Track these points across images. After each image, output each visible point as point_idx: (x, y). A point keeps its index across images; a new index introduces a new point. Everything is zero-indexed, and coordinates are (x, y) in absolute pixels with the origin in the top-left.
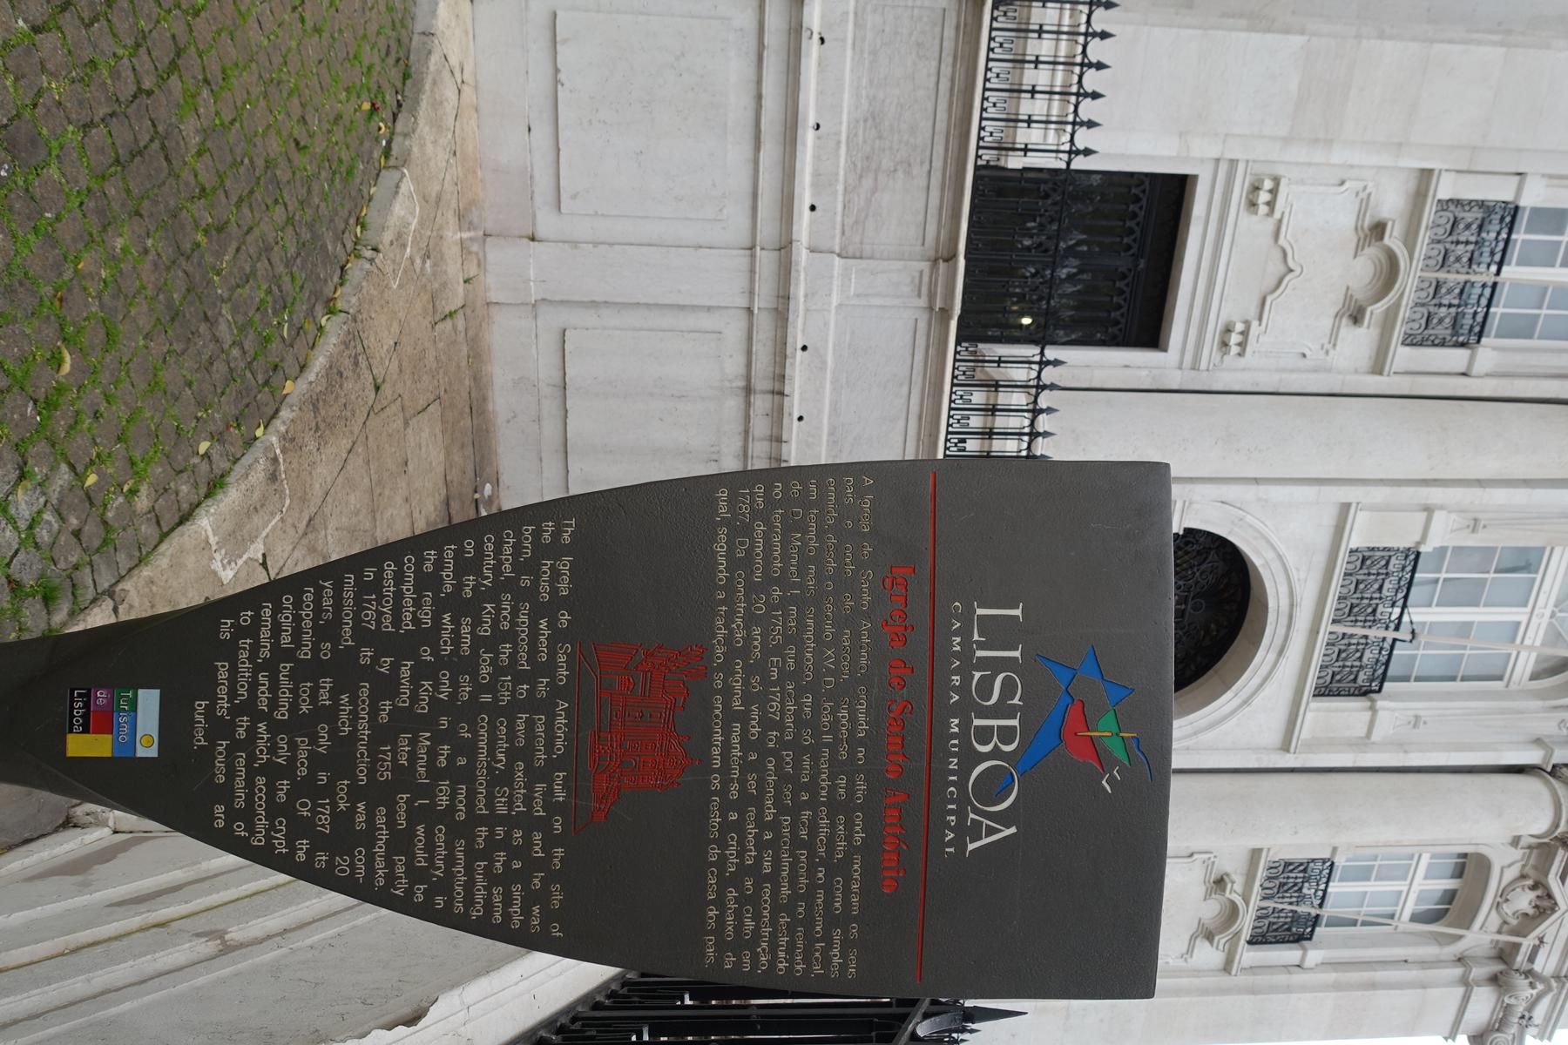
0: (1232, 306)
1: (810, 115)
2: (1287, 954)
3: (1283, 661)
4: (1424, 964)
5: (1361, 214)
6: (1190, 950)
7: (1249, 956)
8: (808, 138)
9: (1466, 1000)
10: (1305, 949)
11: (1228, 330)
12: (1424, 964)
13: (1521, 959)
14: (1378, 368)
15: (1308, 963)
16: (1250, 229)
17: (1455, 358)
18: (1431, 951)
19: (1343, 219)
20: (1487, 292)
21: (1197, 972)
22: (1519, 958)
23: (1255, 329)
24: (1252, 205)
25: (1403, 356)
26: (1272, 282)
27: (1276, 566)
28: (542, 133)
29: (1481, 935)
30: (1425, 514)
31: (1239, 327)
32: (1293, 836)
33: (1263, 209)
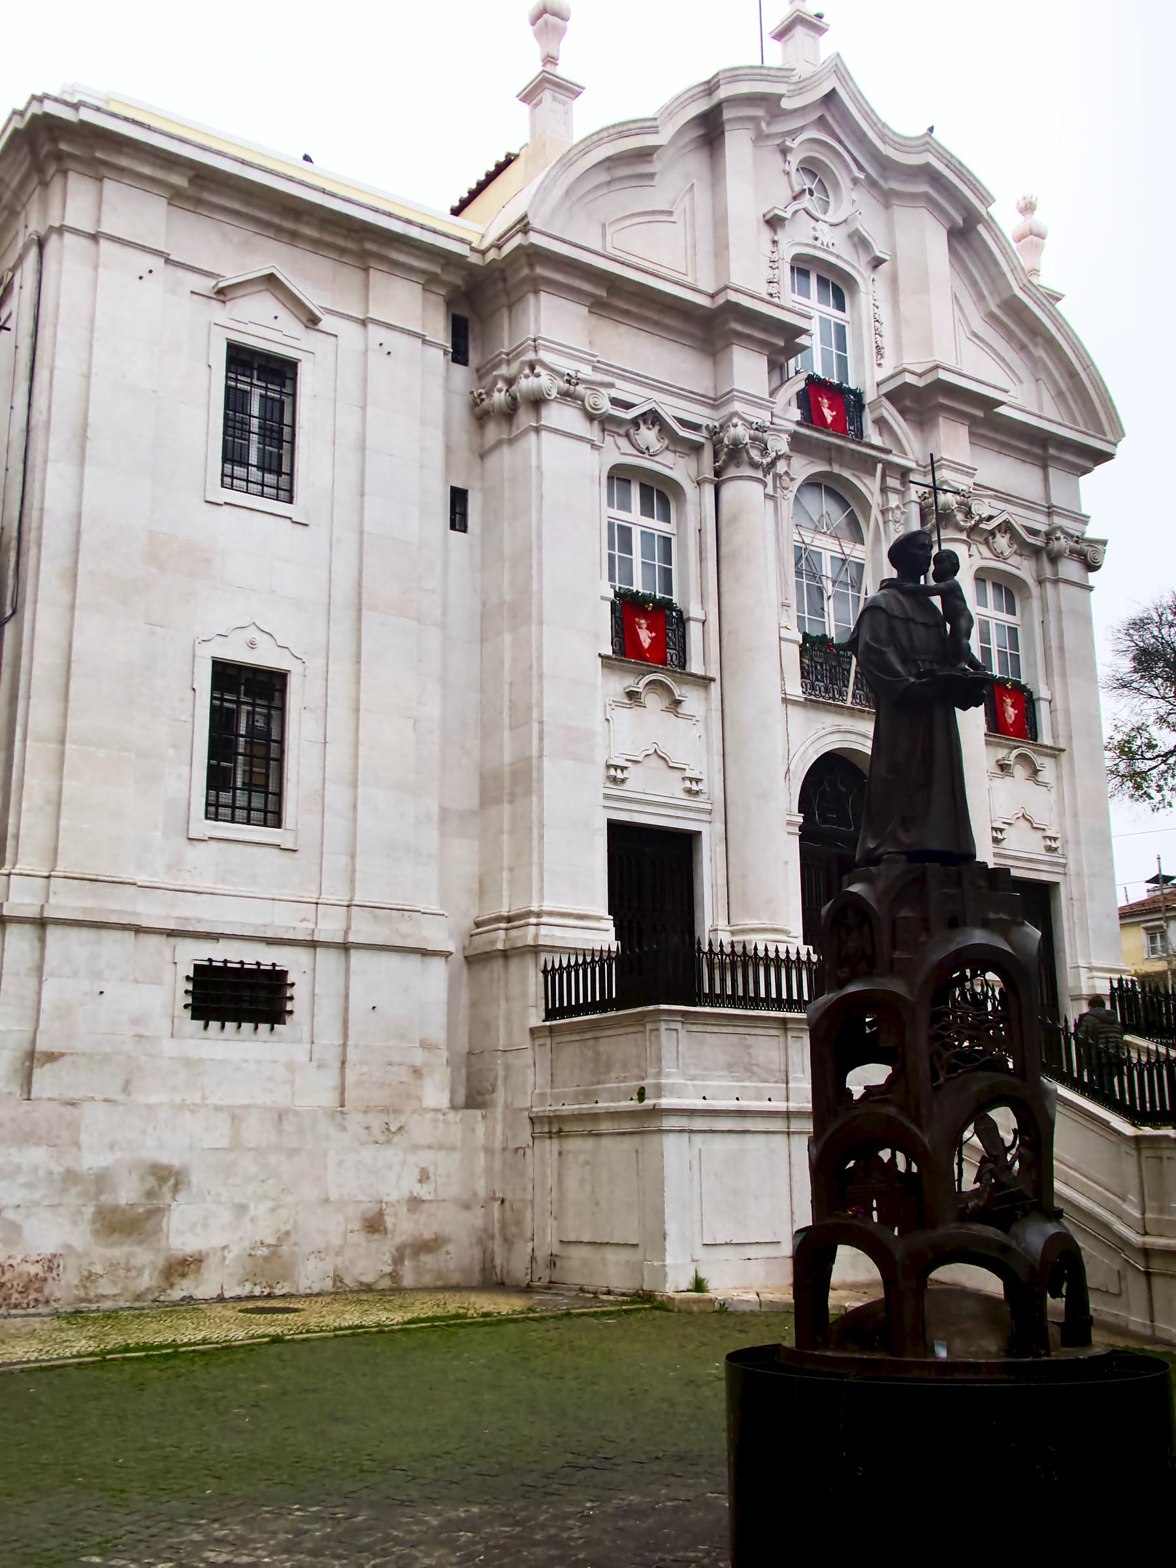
0: (673, 788)
1: (731, 1104)
2: (1043, 710)
4: (1044, 610)
5: (623, 706)
6: (1045, 785)
7: (1046, 738)
8: (745, 1104)
9: (1067, 582)
10: (1039, 699)
11: (689, 791)
12: (1044, 610)
13: (1038, 542)
16: (637, 781)
17: (694, 630)
18: (1035, 604)
19: (625, 717)
21: (1059, 778)
22: (1039, 543)
23: (688, 774)
24: (623, 781)
25: (695, 666)
26: (661, 762)
27: (817, 745)
28: (751, 1252)
29: (1024, 569)
31: (688, 784)
33: (626, 774)
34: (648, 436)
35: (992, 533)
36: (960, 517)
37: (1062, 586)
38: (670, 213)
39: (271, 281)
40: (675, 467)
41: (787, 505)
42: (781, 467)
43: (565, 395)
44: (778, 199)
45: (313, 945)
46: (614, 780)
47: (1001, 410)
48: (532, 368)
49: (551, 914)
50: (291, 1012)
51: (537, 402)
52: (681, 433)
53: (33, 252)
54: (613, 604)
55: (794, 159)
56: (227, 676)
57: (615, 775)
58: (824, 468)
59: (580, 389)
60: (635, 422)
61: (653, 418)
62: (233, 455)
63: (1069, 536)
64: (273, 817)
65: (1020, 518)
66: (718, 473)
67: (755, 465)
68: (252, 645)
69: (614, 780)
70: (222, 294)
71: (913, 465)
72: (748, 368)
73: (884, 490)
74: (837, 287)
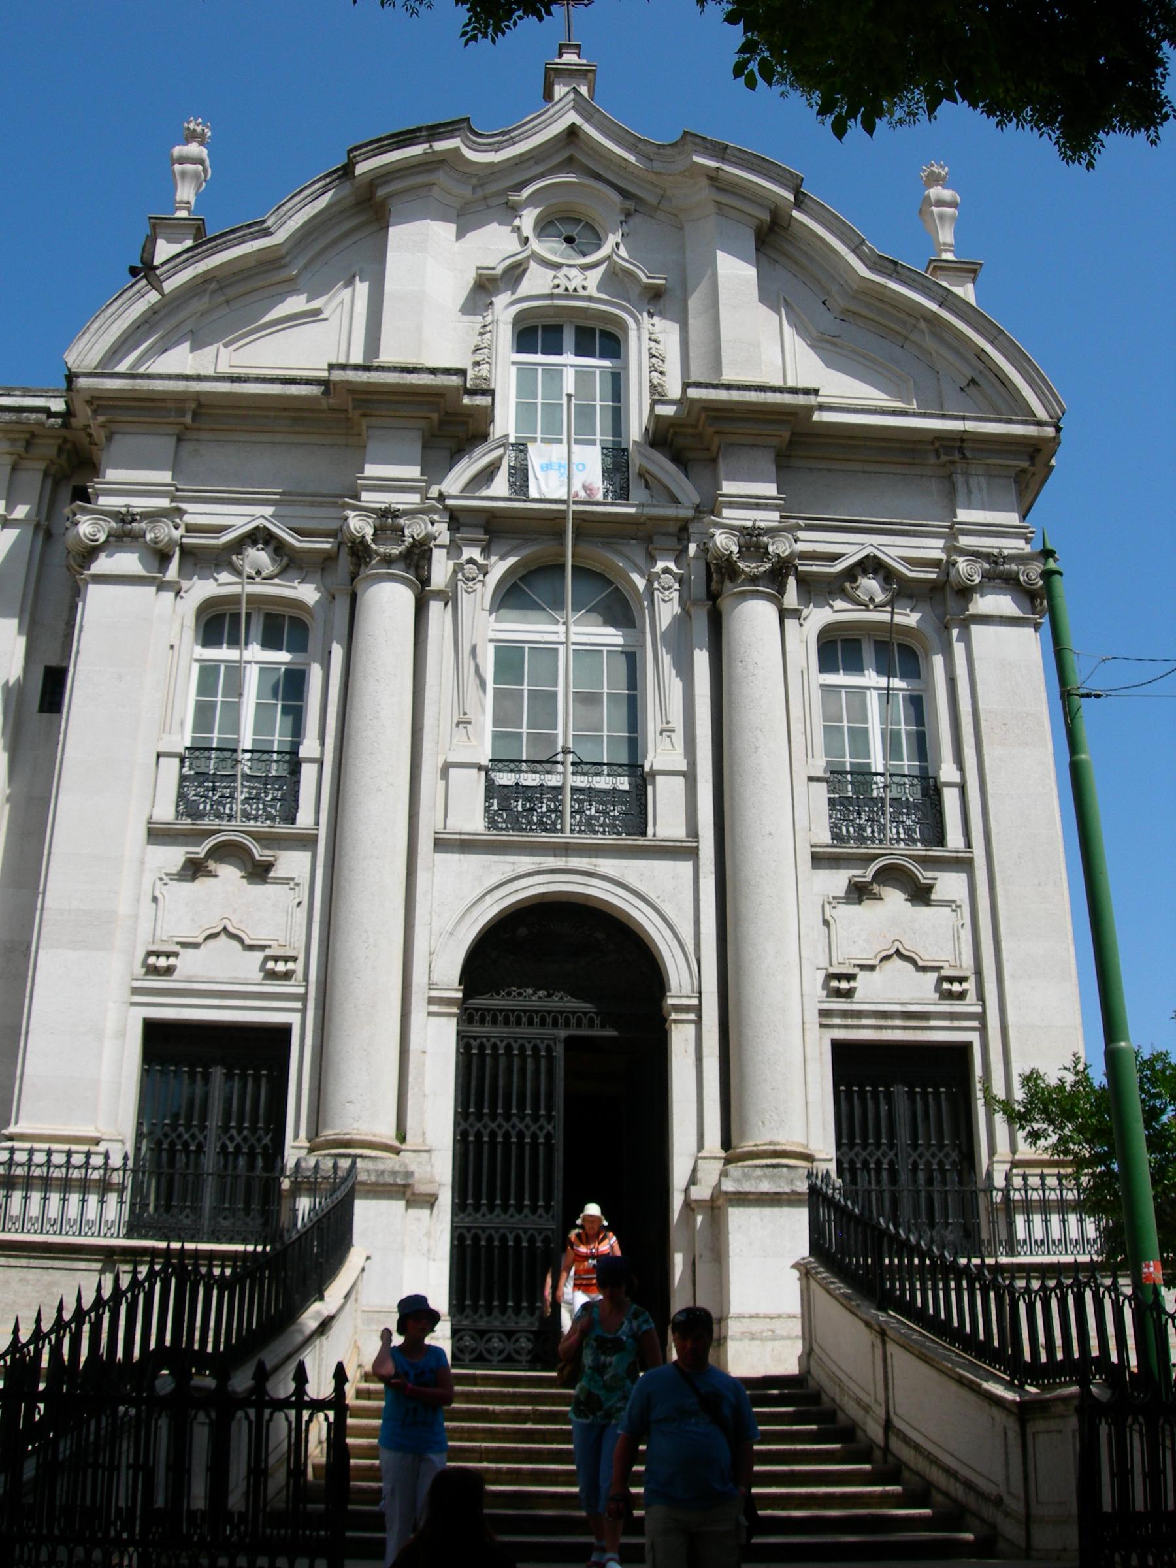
2: (950, 798)
7: (954, 839)
11: (271, 975)
14: (306, 842)
15: (956, 777)
20: (257, 755)
25: (305, 818)
30: (451, 770)
41: (477, 600)
51: (91, 552)
67: (388, 561)
71: (690, 513)
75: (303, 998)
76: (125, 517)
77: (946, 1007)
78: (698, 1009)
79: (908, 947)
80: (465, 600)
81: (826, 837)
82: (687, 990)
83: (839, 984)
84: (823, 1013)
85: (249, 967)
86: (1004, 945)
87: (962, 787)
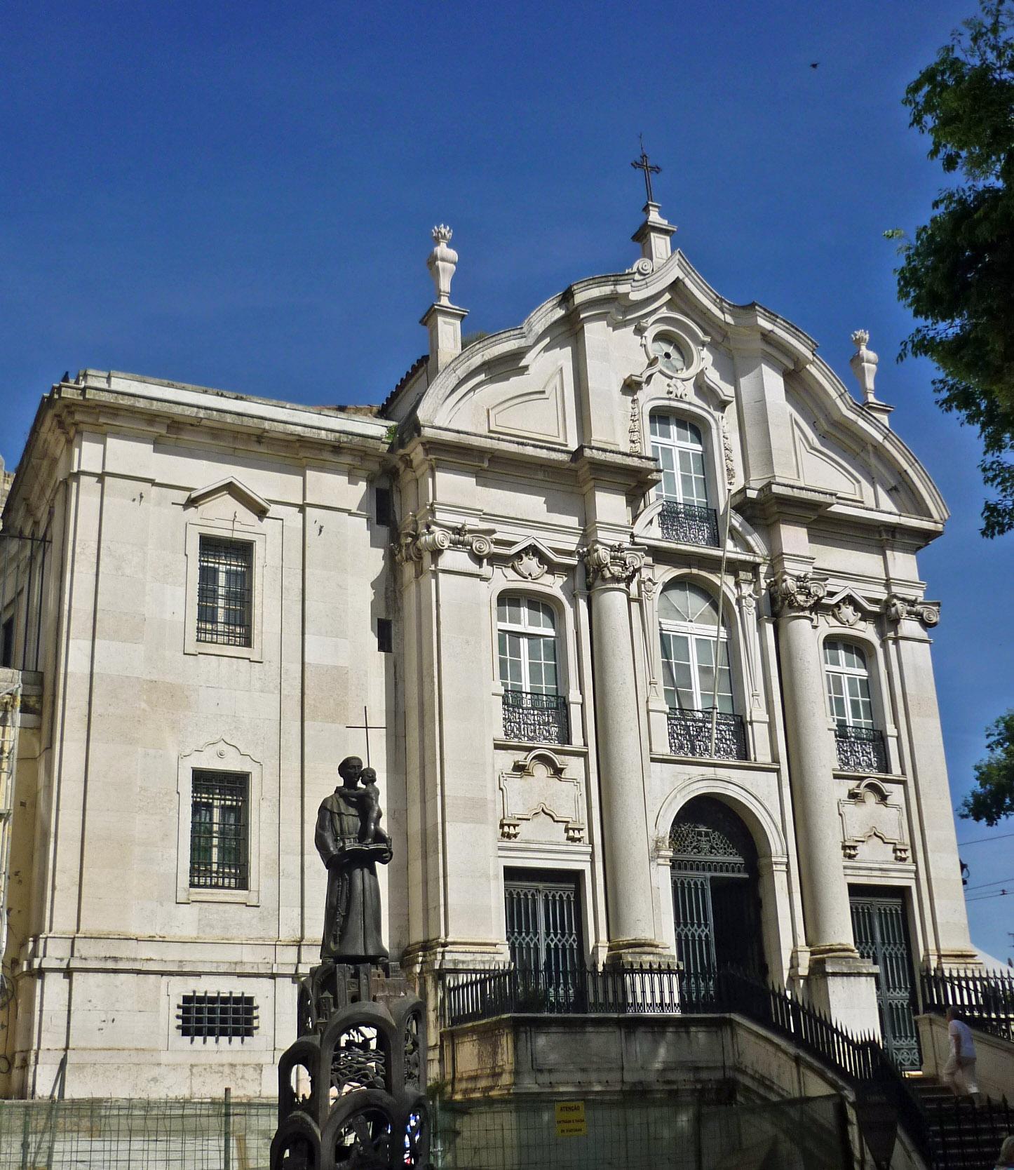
2: (892, 743)
3: (733, 780)
6: (894, 806)
13: (876, 609)
24: (515, 836)
25: (577, 741)
29: (868, 631)
32: (824, 752)
34: (530, 564)
35: (837, 605)
36: (801, 598)
37: (901, 642)
38: (543, 392)
39: (231, 488)
40: (553, 585)
42: (646, 574)
43: (455, 543)
44: (637, 367)
45: (273, 976)
46: (509, 836)
47: (832, 509)
48: (428, 527)
49: (454, 943)
50: (257, 1028)
51: (437, 553)
52: (556, 560)
53: (62, 489)
54: (505, 697)
55: (650, 333)
56: (203, 779)
57: (507, 831)
58: (686, 571)
59: (468, 537)
60: (518, 556)
61: (533, 550)
62: (206, 614)
63: (903, 600)
64: (243, 884)
65: (861, 592)
66: (589, 587)
67: (617, 579)
68: (221, 755)
69: (509, 836)
70: (192, 502)
72: (610, 506)
73: (737, 585)
74: (696, 427)
75: (592, 855)
76: (458, 531)
77: (900, 866)
78: (788, 865)
79: (880, 831)
80: (648, 605)
81: (837, 765)
82: (780, 853)
83: (849, 850)
84: (845, 868)
85: (559, 833)
86: (927, 832)
87: (898, 738)
